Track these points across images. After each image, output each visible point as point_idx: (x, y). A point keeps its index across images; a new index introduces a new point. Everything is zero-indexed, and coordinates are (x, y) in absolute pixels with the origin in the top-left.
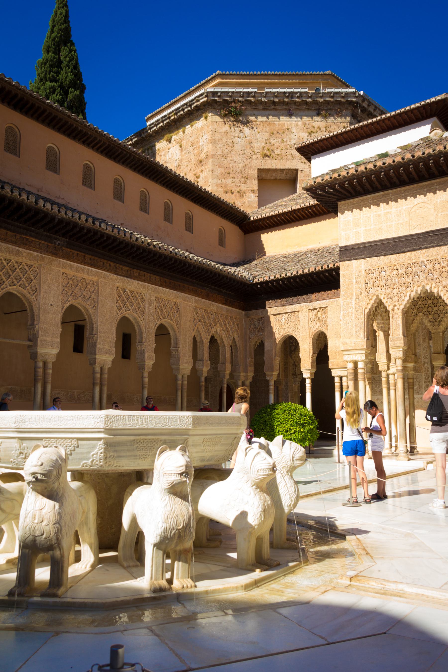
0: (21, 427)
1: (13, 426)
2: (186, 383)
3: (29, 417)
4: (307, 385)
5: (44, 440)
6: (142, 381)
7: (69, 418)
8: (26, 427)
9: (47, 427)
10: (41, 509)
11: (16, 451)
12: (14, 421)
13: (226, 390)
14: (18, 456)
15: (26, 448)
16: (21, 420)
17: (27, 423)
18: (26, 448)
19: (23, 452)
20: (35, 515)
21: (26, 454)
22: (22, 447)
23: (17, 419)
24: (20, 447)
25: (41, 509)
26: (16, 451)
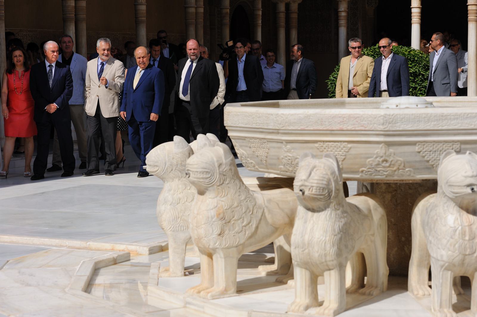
0: (391, 129)
1: (381, 127)
2: (201, 10)
3: (401, 117)
4: (413, 10)
5: (417, 144)
6: (136, 11)
7: (452, 117)
8: (398, 129)
9: (425, 128)
10: (471, 225)
11: (376, 158)
12: (382, 121)
13: (260, 22)
14: (378, 164)
15: (392, 155)
16: (391, 120)
17: (399, 124)
18: (392, 155)
19: (388, 159)
20: (465, 232)
21: (391, 161)
22: (387, 154)
23: (385, 119)
24: (385, 154)
25: (471, 225)
26: (376, 158)
